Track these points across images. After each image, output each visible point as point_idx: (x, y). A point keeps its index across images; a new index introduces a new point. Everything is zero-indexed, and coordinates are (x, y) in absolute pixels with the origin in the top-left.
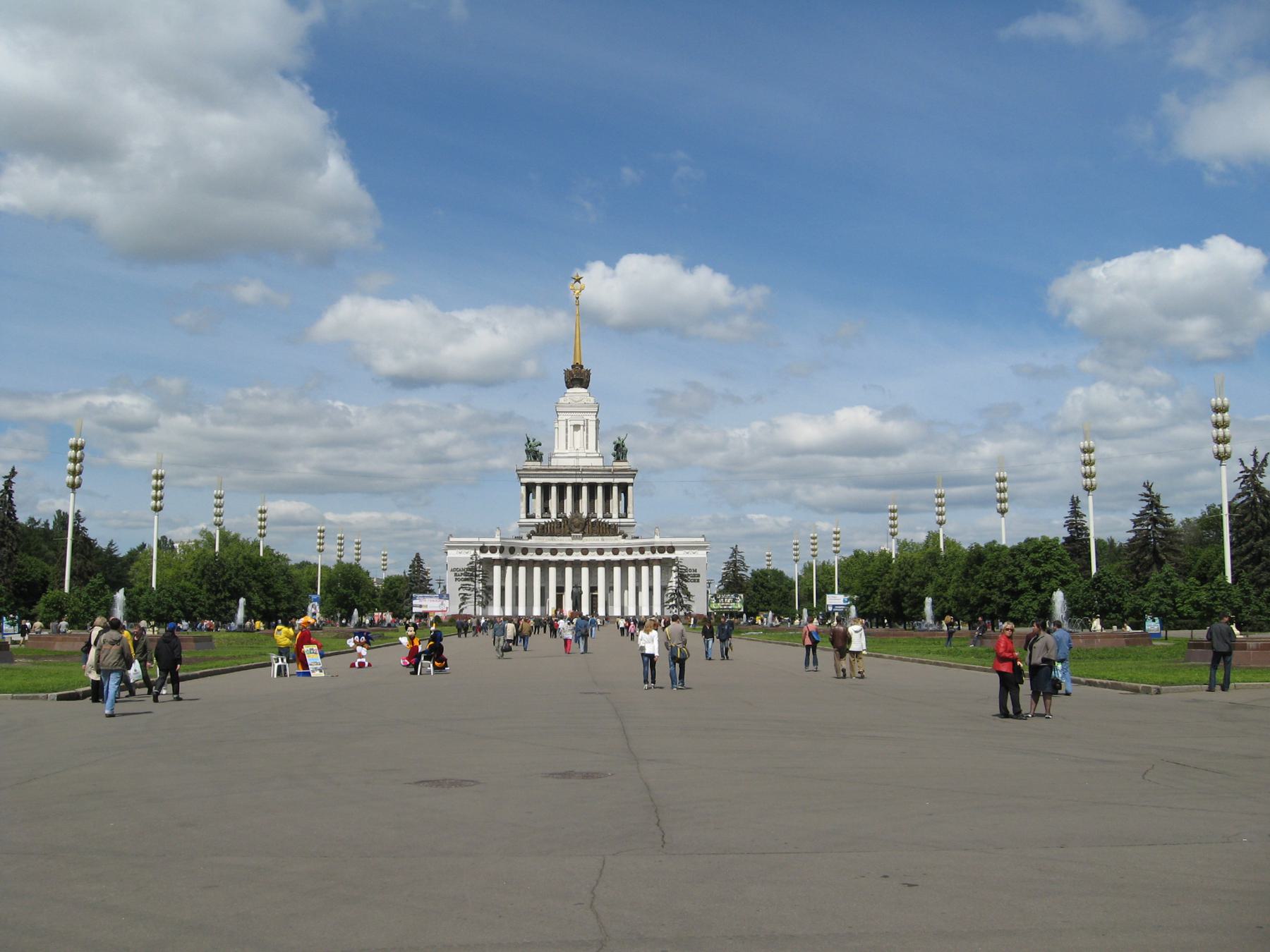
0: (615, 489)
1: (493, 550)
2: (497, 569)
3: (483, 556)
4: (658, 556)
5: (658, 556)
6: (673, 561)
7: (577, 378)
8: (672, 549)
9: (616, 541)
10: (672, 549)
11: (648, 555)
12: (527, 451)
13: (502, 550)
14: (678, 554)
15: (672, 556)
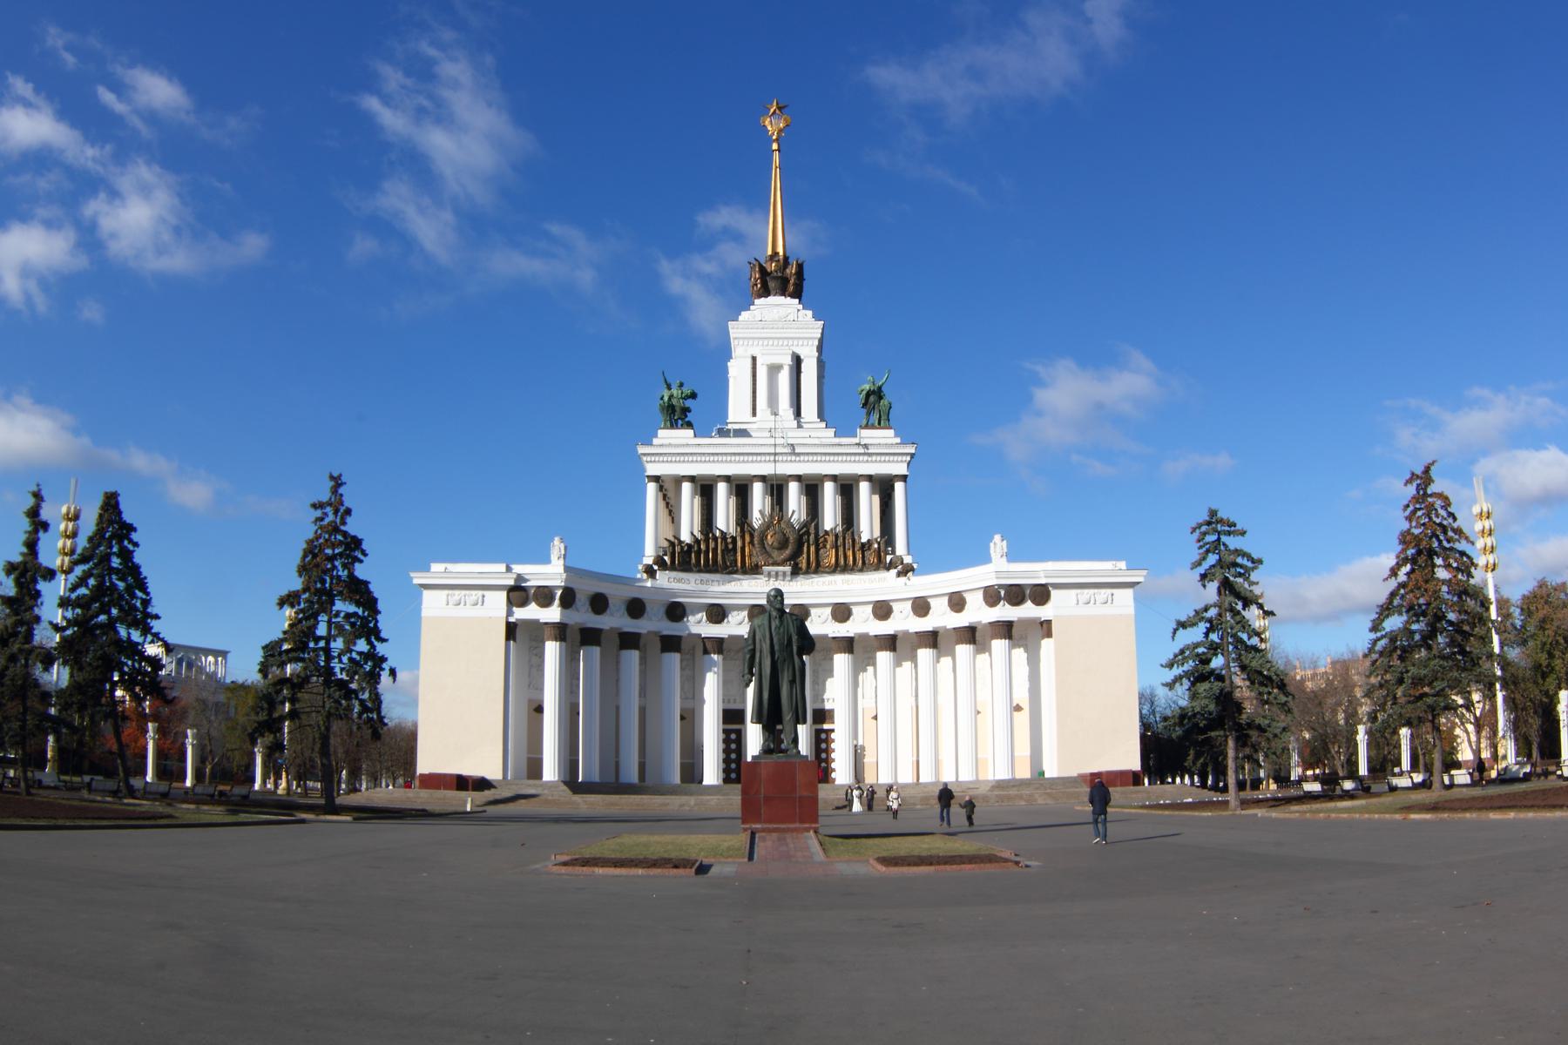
0: (864, 487)
1: (544, 596)
2: (552, 649)
3: (520, 614)
4: (1005, 612)
5: (1005, 612)
6: (1046, 628)
7: (781, 279)
8: (1041, 594)
9: (881, 584)
10: (1041, 594)
11: (978, 613)
12: (663, 408)
13: (568, 598)
14: (1058, 607)
15: (1043, 612)
